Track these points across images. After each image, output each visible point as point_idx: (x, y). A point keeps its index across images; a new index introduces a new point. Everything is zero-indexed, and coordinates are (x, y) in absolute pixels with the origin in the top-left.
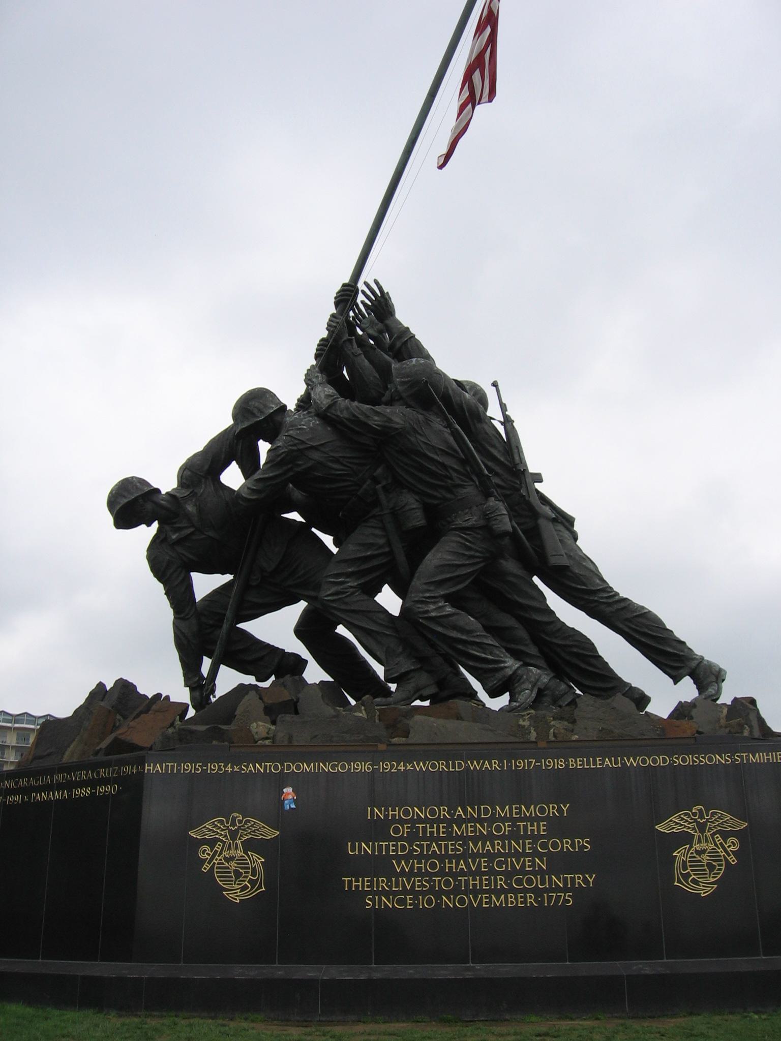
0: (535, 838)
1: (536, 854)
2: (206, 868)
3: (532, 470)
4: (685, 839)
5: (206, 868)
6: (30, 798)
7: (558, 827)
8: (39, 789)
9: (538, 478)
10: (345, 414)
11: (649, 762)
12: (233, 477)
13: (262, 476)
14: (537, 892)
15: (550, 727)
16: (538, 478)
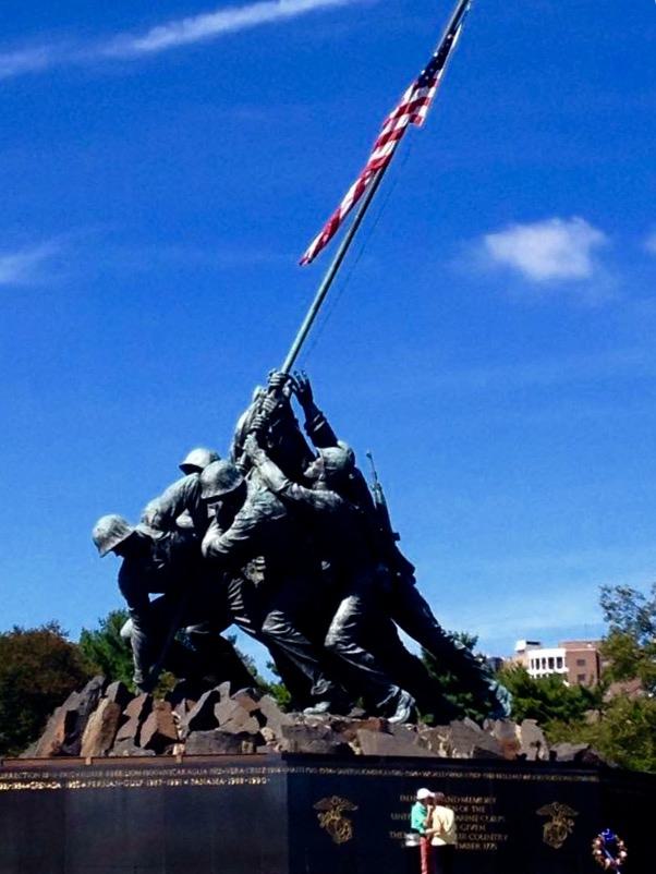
0: (480, 814)
1: (480, 823)
2: (322, 825)
3: (394, 530)
4: (549, 819)
5: (322, 825)
6: (190, 781)
7: (490, 810)
8: (198, 777)
9: (397, 537)
10: (297, 497)
11: (534, 777)
12: (184, 520)
13: (233, 538)
14: (481, 842)
15: (440, 741)
16: (397, 537)
